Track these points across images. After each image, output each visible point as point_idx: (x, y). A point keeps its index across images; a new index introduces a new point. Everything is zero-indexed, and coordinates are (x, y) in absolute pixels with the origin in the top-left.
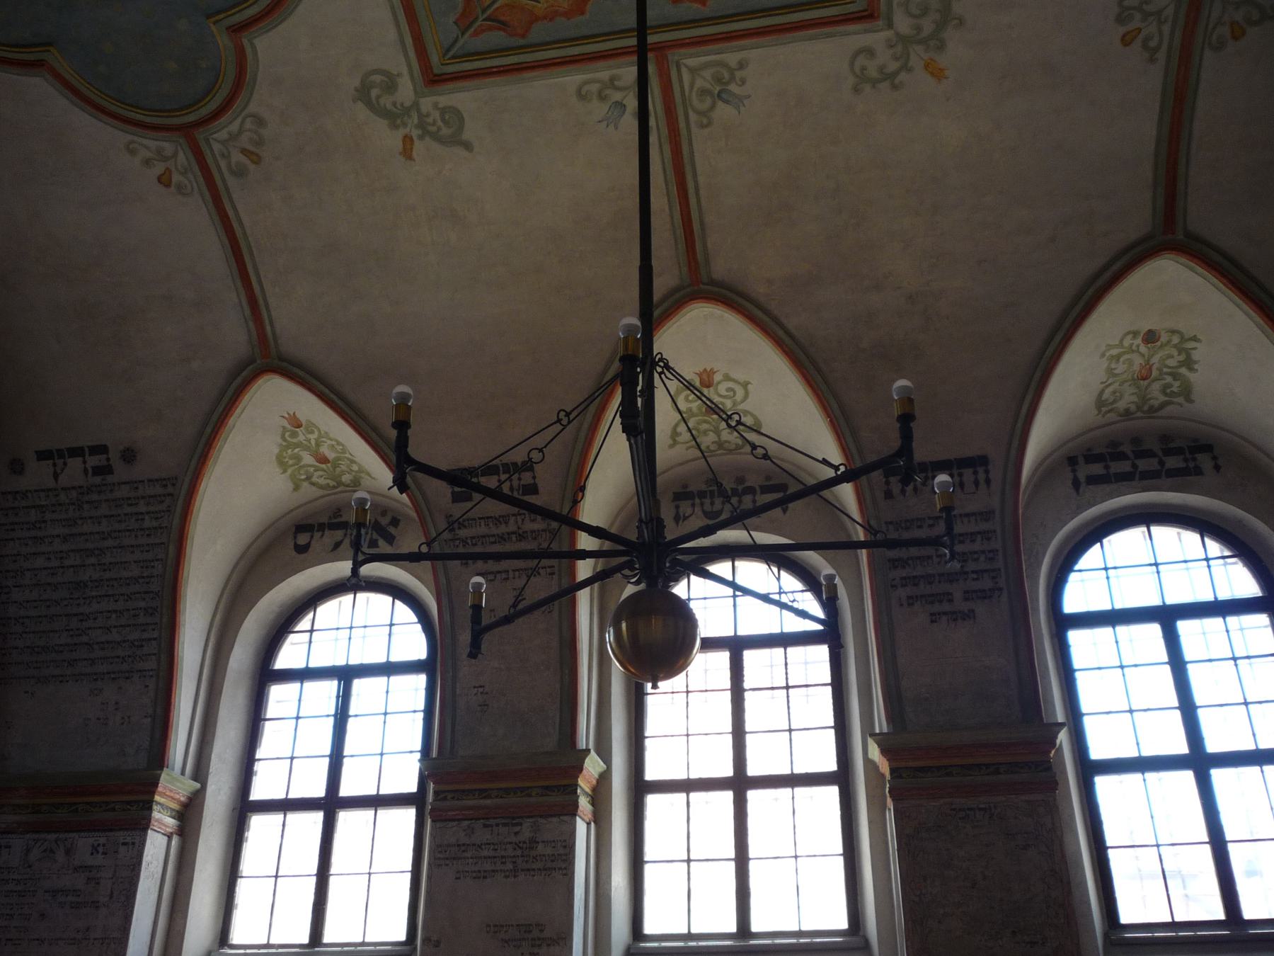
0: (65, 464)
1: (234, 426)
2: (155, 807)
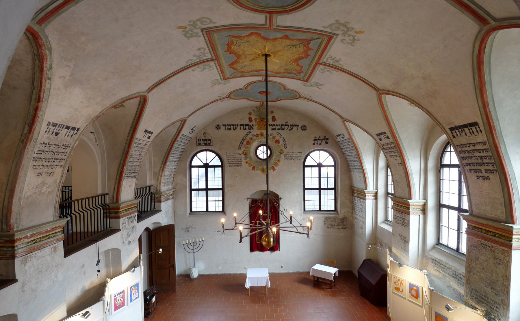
1: (350, 128)
2: (366, 196)
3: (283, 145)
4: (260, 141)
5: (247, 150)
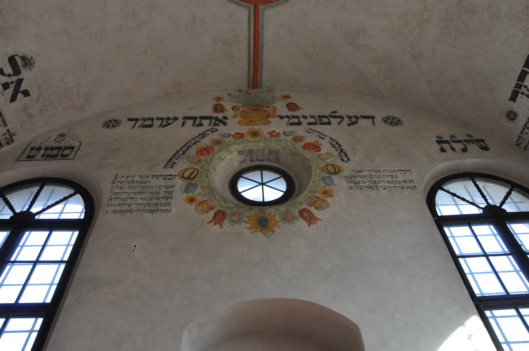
0: (526, 87)
3: (336, 153)
4: (251, 151)
5: (197, 167)
